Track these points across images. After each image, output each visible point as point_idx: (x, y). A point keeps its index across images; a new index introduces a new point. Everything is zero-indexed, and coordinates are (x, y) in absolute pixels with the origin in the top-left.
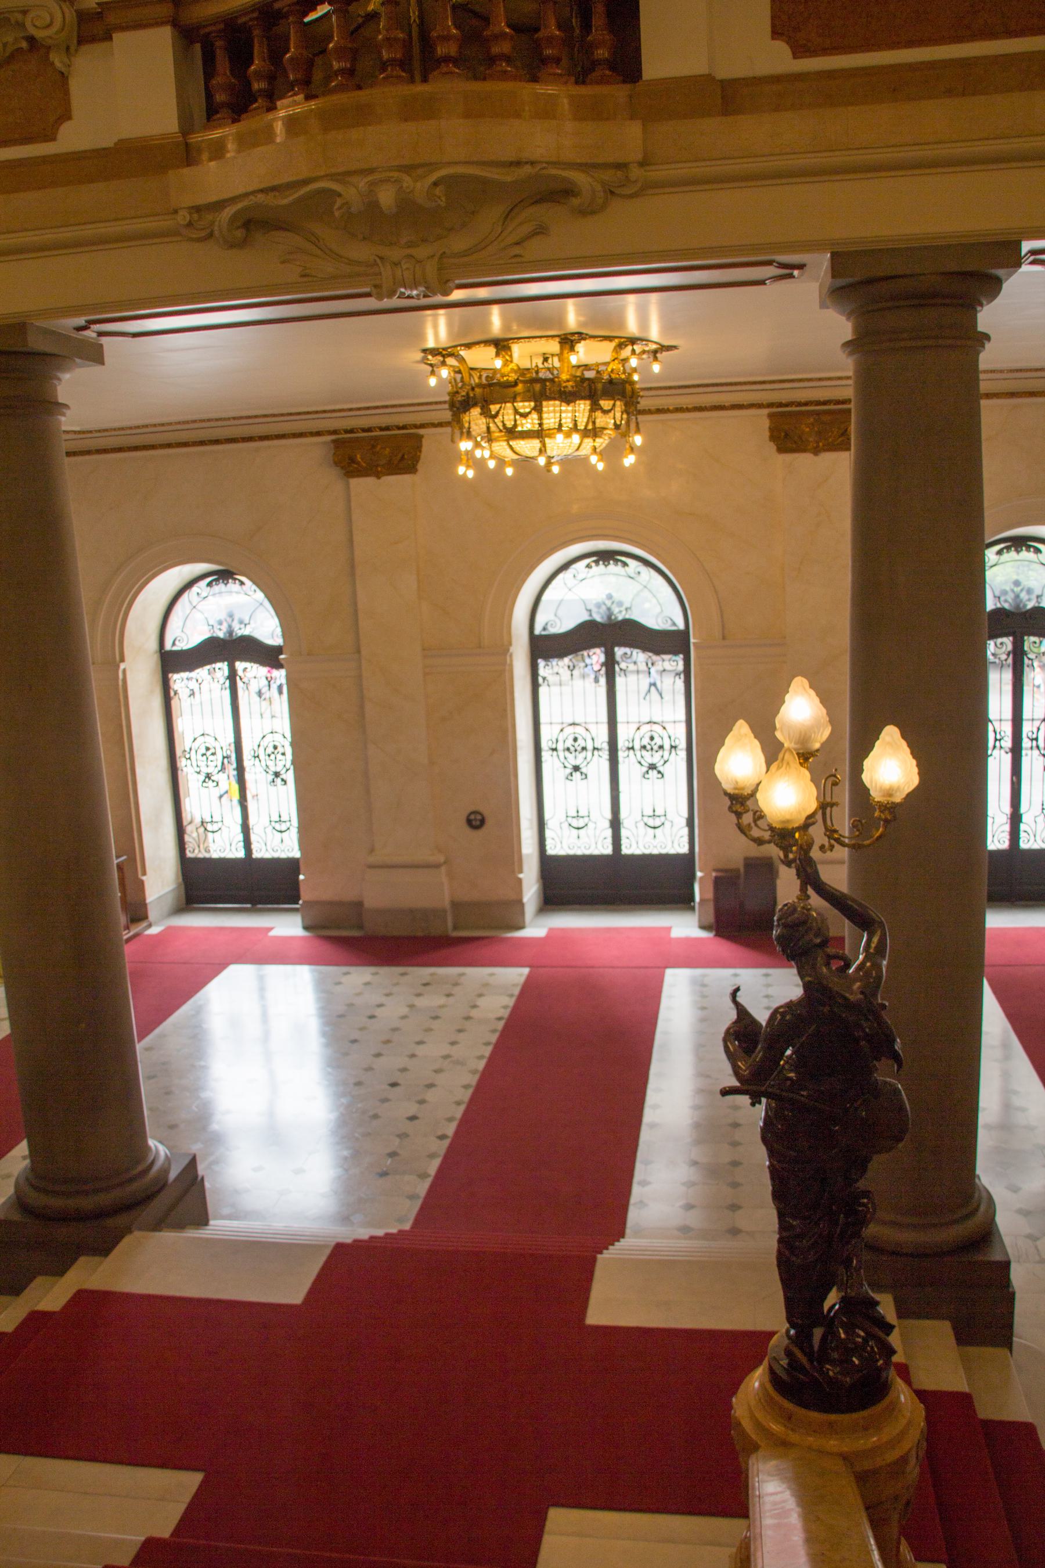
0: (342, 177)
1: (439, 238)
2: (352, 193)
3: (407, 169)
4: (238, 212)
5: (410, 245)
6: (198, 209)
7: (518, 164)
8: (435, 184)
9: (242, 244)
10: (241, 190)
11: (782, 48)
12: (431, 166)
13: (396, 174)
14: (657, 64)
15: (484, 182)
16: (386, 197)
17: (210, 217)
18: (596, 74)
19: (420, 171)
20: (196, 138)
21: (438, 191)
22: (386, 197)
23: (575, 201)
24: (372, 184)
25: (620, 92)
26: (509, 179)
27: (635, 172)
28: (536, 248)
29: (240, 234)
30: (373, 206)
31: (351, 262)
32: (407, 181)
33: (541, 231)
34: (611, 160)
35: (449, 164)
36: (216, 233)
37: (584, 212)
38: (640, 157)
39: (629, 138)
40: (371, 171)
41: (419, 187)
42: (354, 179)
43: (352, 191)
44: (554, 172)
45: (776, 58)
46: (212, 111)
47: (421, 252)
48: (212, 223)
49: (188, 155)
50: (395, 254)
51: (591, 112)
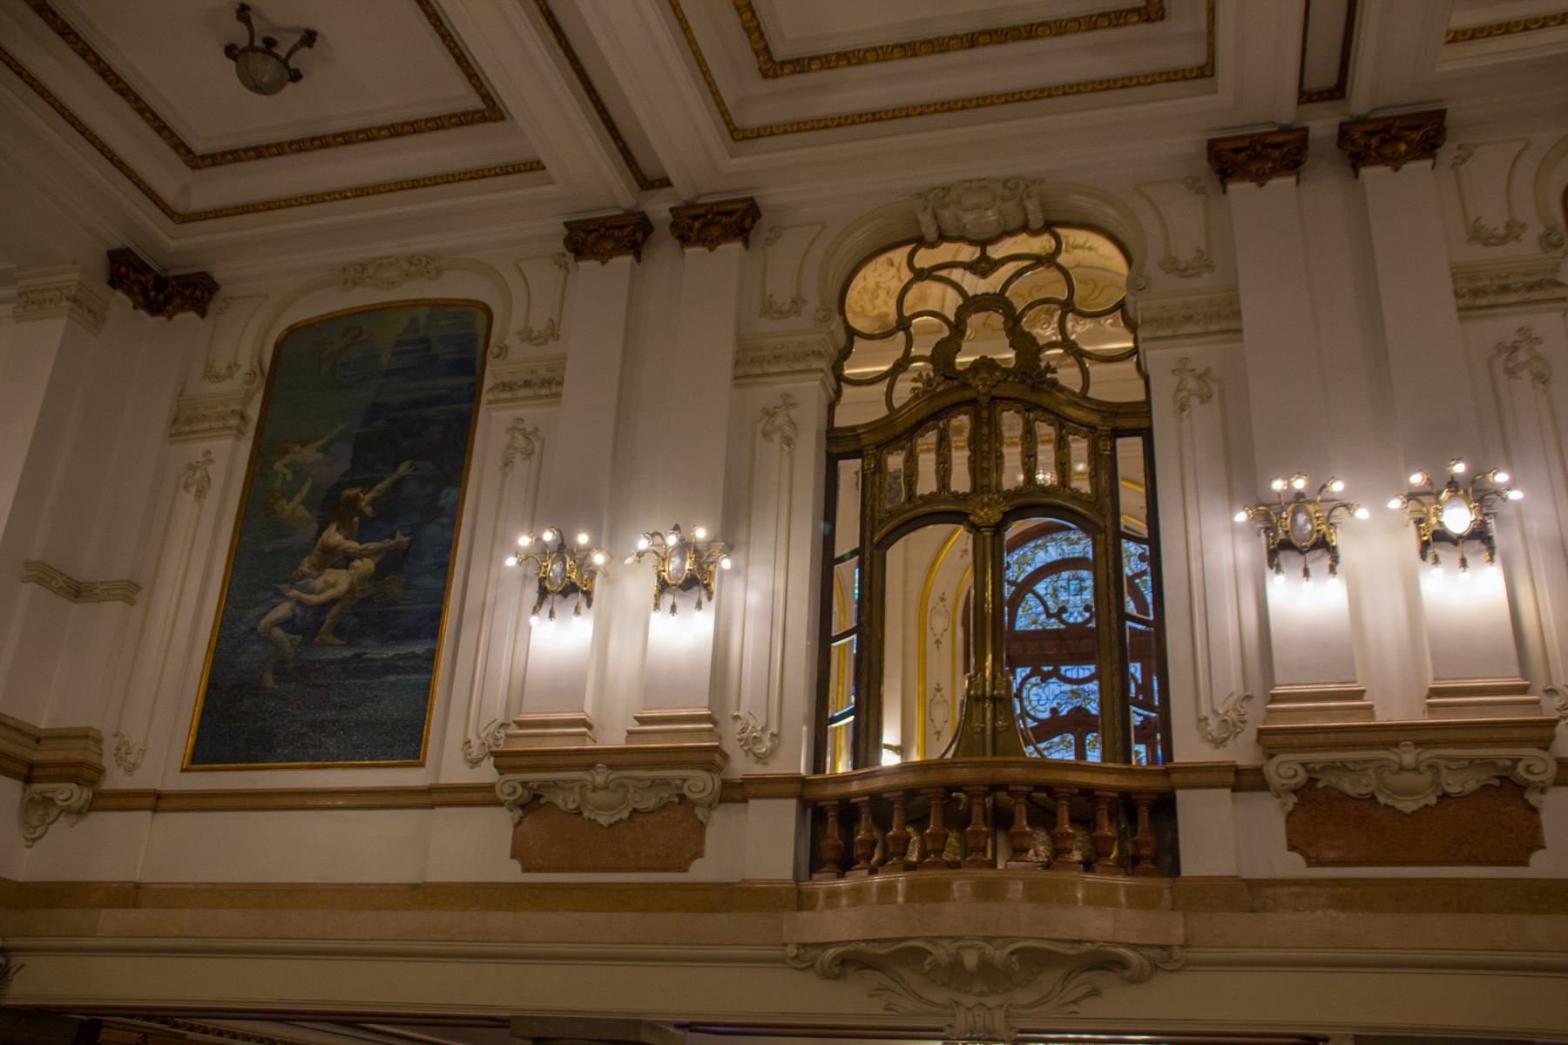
0: (933, 940)
1: (1007, 991)
2: (942, 953)
3: (988, 939)
4: (842, 954)
5: (982, 994)
6: (804, 946)
7: (1080, 941)
8: (1012, 953)
9: (836, 977)
10: (845, 938)
11: (1297, 858)
12: (1011, 939)
13: (980, 943)
14: (1193, 864)
15: (1050, 952)
16: (971, 960)
17: (814, 953)
18: (1142, 866)
19: (999, 942)
20: (806, 886)
21: (1014, 958)
22: (971, 960)
23: (1127, 974)
24: (960, 948)
25: (1164, 883)
26: (1072, 952)
27: (1178, 953)
28: (1089, 1008)
29: (837, 970)
30: (956, 966)
31: (934, 1004)
32: (989, 949)
33: (1095, 992)
34: (1157, 942)
35: (1024, 938)
36: (818, 966)
37: (1133, 981)
38: (1182, 942)
39: (1174, 928)
40: (959, 938)
41: (999, 955)
42: (945, 943)
43: (942, 951)
44: (1109, 949)
45: (1293, 865)
46: (816, 864)
47: (991, 1001)
48: (816, 957)
49: (803, 901)
50: (969, 1000)
51: (1139, 900)
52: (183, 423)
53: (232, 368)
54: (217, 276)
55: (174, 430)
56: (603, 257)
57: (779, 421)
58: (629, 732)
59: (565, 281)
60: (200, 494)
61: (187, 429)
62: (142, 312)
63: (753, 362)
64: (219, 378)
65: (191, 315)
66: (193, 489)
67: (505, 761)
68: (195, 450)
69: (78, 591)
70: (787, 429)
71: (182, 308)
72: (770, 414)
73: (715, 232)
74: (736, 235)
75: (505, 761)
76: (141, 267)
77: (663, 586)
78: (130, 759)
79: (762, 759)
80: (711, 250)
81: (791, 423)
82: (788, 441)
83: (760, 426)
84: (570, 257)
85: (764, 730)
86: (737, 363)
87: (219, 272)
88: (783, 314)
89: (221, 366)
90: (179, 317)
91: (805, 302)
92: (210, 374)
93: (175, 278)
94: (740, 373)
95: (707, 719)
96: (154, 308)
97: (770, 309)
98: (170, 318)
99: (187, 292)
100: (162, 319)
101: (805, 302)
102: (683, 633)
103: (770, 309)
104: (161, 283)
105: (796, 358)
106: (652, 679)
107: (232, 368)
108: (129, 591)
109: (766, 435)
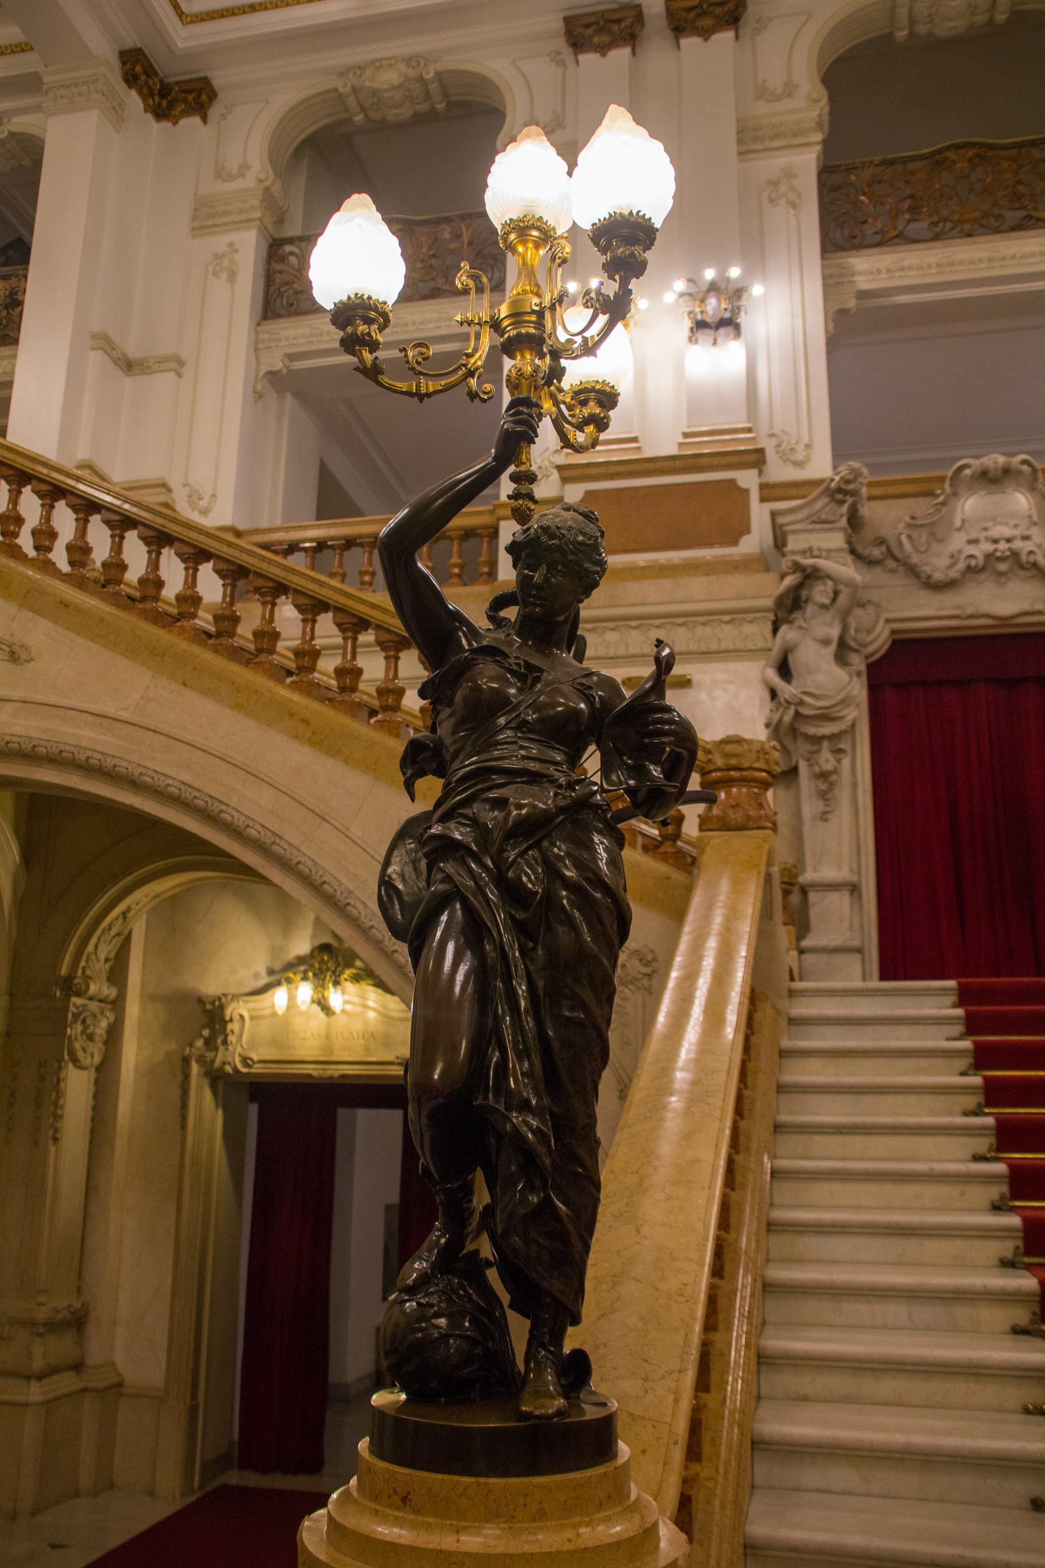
52: (206, 218)
53: (244, 168)
54: (216, 83)
55: (196, 224)
56: (603, 49)
57: (783, 188)
58: (680, 444)
59: (564, 74)
60: (232, 276)
61: (210, 223)
62: (150, 117)
63: (755, 140)
64: (232, 178)
65: (196, 120)
66: (224, 275)
67: (569, 473)
68: (219, 242)
69: (129, 366)
70: (791, 196)
71: (185, 114)
72: (775, 184)
73: (707, 22)
74: (728, 23)
75: (569, 473)
76: (150, 72)
77: (700, 325)
78: (203, 504)
79: (799, 464)
80: (706, 39)
81: (793, 189)
82: (793, 205)
83: (765, 194)
84: (567, 52)
85: (797, 442)
86: (740, 141)
87: (219, 79)
88: (779, 98)
89: (232, 165)
90: (184, 122)
91: (797, 86)
92: (220, 174)
93: (177, 83)
94: (745, 148)
95: (749, 430)
96: (160, 114)
97: (762, 92)
98: (175, 124)
99: (190, 98)
100: (166, 125)
101: (797, 86)
102: (721, 362)
103: (762, 92)
104: (165, 90)
105: (795, 135)
106: (696, 401)
107: (244, 168)
108: (176, 364)
109: (772, 201)
